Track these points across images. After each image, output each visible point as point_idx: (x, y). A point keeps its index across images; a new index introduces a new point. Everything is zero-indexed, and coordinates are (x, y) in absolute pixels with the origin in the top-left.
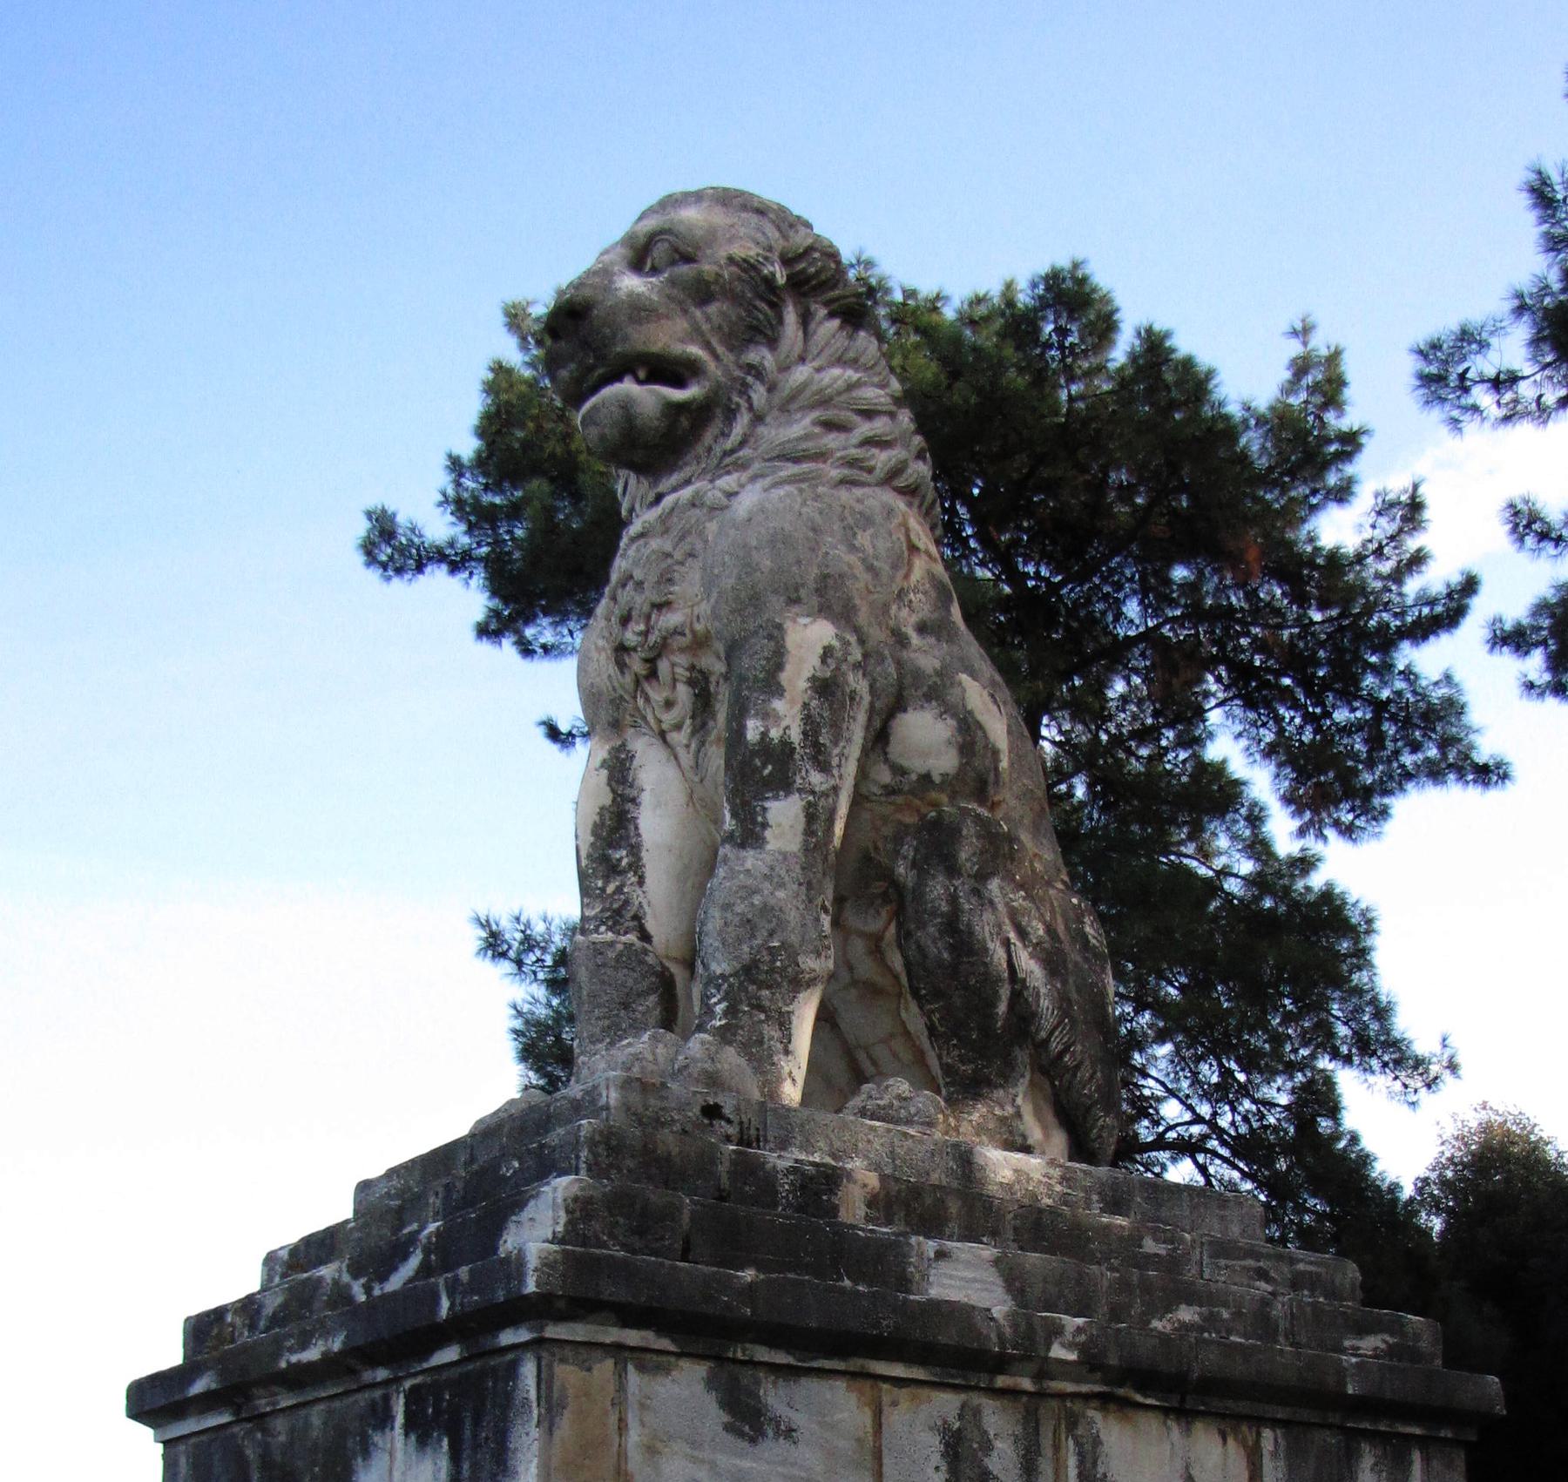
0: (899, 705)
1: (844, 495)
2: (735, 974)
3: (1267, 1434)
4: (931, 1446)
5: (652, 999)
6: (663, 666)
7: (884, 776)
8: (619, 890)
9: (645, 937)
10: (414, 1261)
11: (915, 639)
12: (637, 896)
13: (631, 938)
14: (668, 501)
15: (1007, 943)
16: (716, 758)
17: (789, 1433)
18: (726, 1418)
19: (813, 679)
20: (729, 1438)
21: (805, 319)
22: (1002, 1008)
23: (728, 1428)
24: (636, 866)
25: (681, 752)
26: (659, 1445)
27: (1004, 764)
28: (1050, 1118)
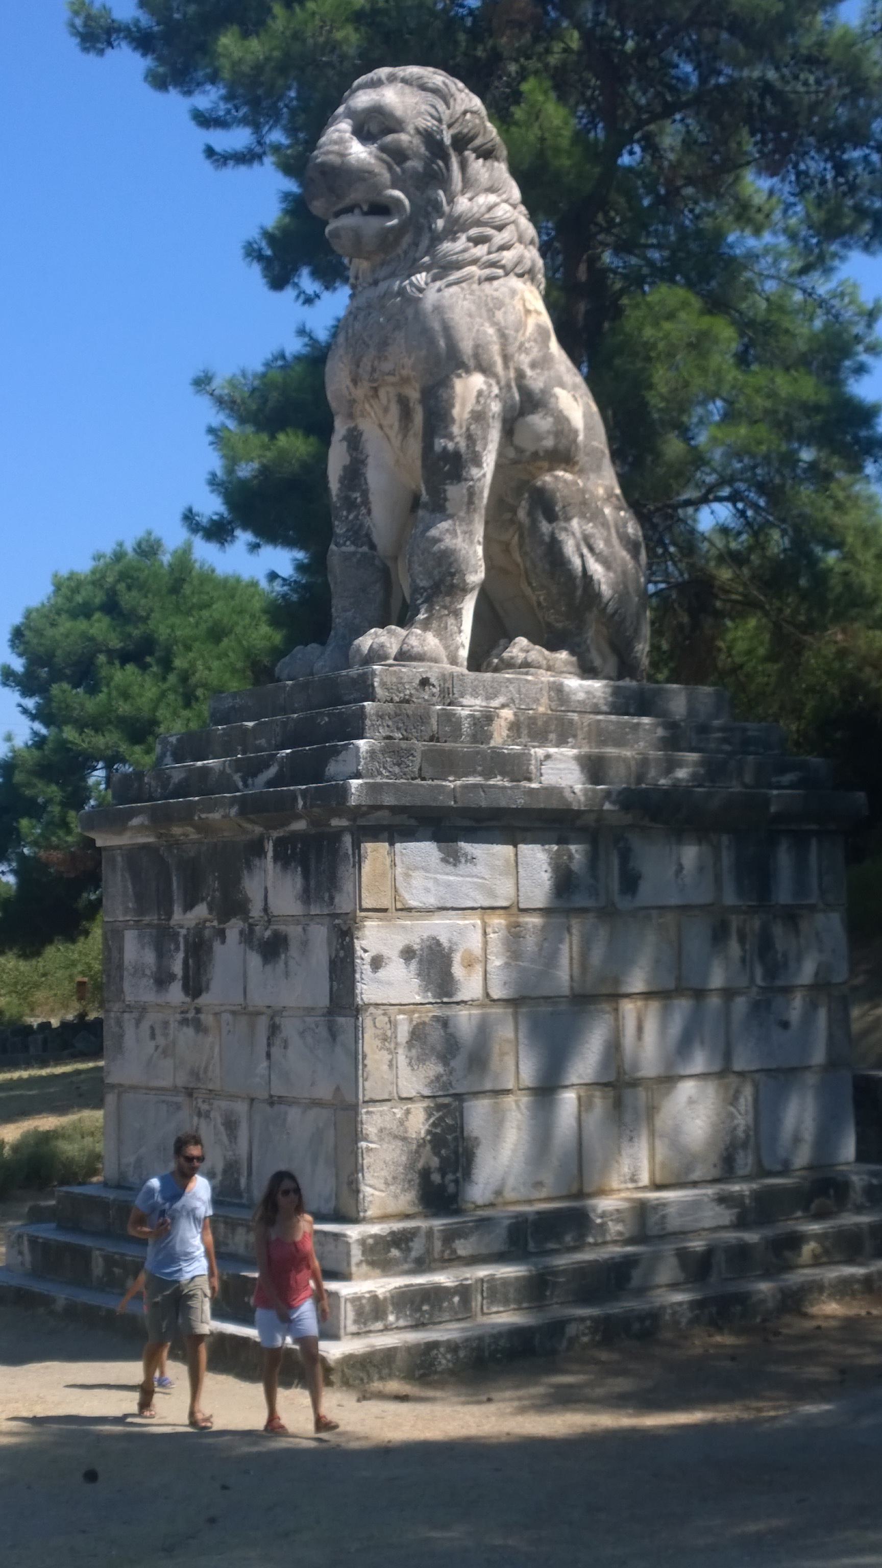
1: (486, 286)
2: (431, 588)
5: (378, 585)
6: (382, 393)
7: (511, 453)
8: (356, 517)
9: (373, 547)
10: (273, 771)
12: (367, 522)
13: (365, 549)
14: (383, 286)
15: (582, 556)
16: (415, 447)
18: (442, 855)
19: (472, 412)
20: (443, 865)
21: (464, 166)
22: (579, 593)
23: (444, 860)
24: (366, 502)
25: (393, 440)
26: (411, 872)
27: (581, 437)
28: (607, 649)
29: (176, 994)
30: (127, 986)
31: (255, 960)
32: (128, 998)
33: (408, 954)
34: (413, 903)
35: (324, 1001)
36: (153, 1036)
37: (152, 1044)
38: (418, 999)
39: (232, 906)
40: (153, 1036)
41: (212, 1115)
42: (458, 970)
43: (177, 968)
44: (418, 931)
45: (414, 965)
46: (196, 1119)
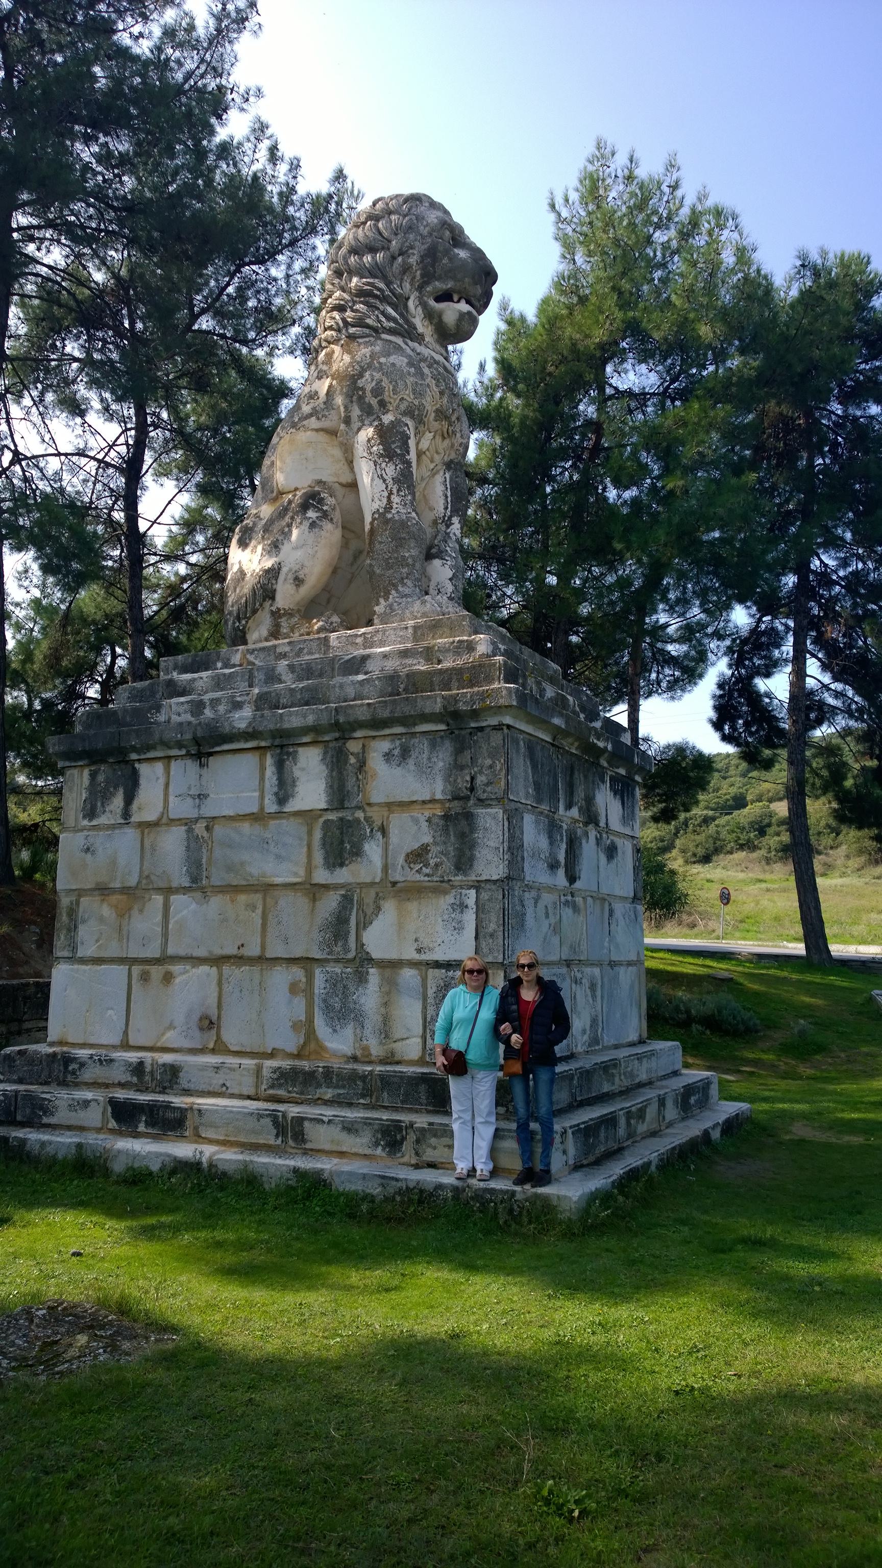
29: (560, 878)
30: (526, 865)
31: (603, 858)
32: (527, 878)
35: (632, 895)
36: (547, 916)
37: (546, 923)
39: (591, 817)
40: (547, 916)
41: (584, 981)
43: (561, 857)
46: (574, 985)
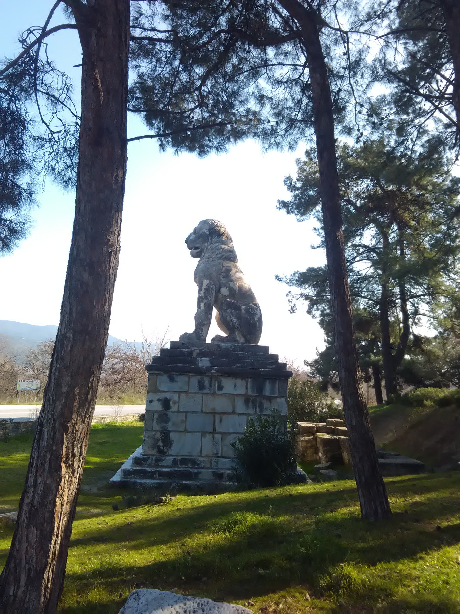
0: (220, 287)
3: (250, 380)
4: (196, 383)
11: (222, 279)
17: (177, 381)
33: (159, 400)
34: (161, 390)
38: (161, 409)
42: (171, 404)
44: (162, 396)
45: (160, 402)
